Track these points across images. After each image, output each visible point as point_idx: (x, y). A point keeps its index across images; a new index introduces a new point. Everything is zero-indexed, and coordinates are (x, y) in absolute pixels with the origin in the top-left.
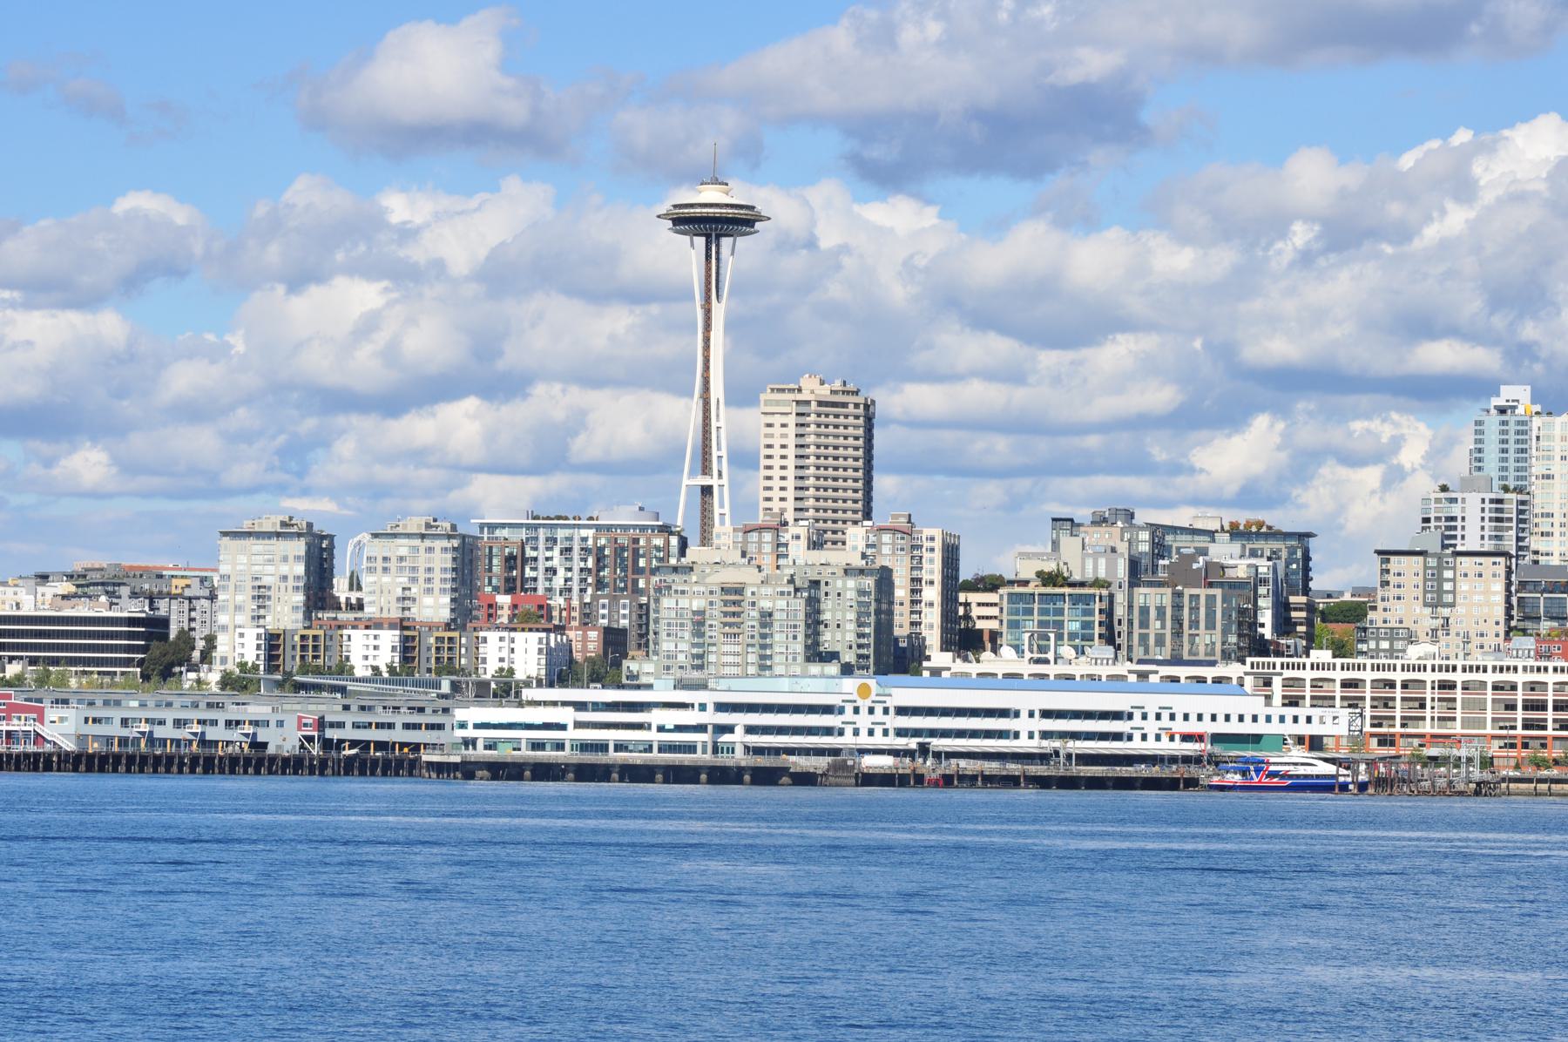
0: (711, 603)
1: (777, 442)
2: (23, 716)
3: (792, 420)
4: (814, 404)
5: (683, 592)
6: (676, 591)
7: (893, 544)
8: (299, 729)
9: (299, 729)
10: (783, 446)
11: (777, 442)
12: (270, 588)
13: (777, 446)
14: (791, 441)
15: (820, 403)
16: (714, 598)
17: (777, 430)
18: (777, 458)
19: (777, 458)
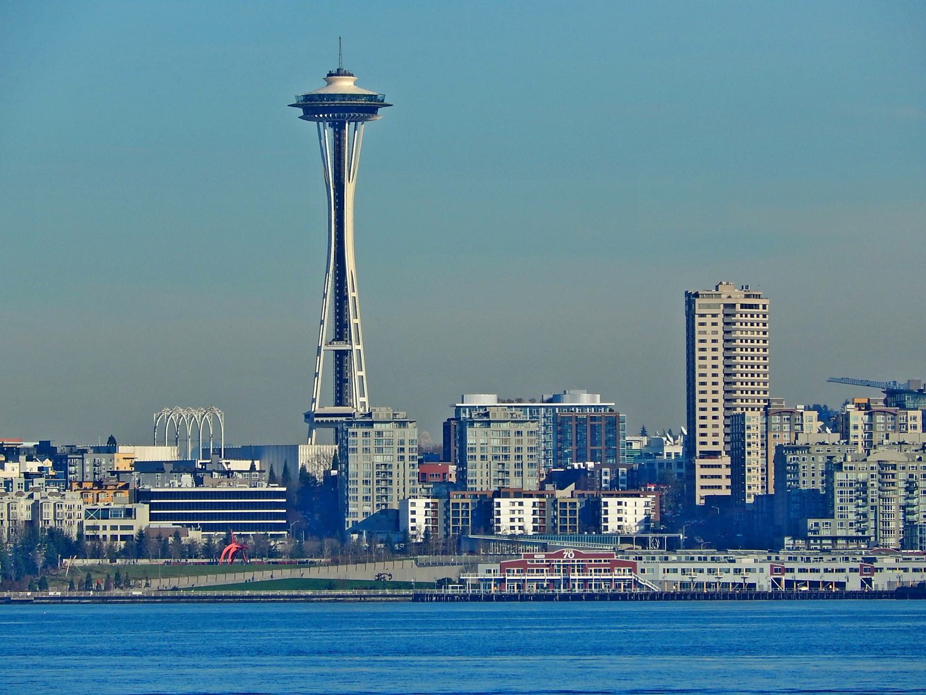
0: (872, 476)
1: (709, 337)
2: (622, 569)
3: (719, 320)
4: (738, 306)
5: (851, 468)
6: (846, 468)
7: (885, 423)
8: (772, 574)
9: (772, 574)
10: (714, 341)
11: (709, 337)
12: (391, 466)
13: (709, 341)
14: (720, 337)
15: (743, 306)
16: (875, 473)
17: (709, 328)
18: (709, 350)
19: (709, 350)
